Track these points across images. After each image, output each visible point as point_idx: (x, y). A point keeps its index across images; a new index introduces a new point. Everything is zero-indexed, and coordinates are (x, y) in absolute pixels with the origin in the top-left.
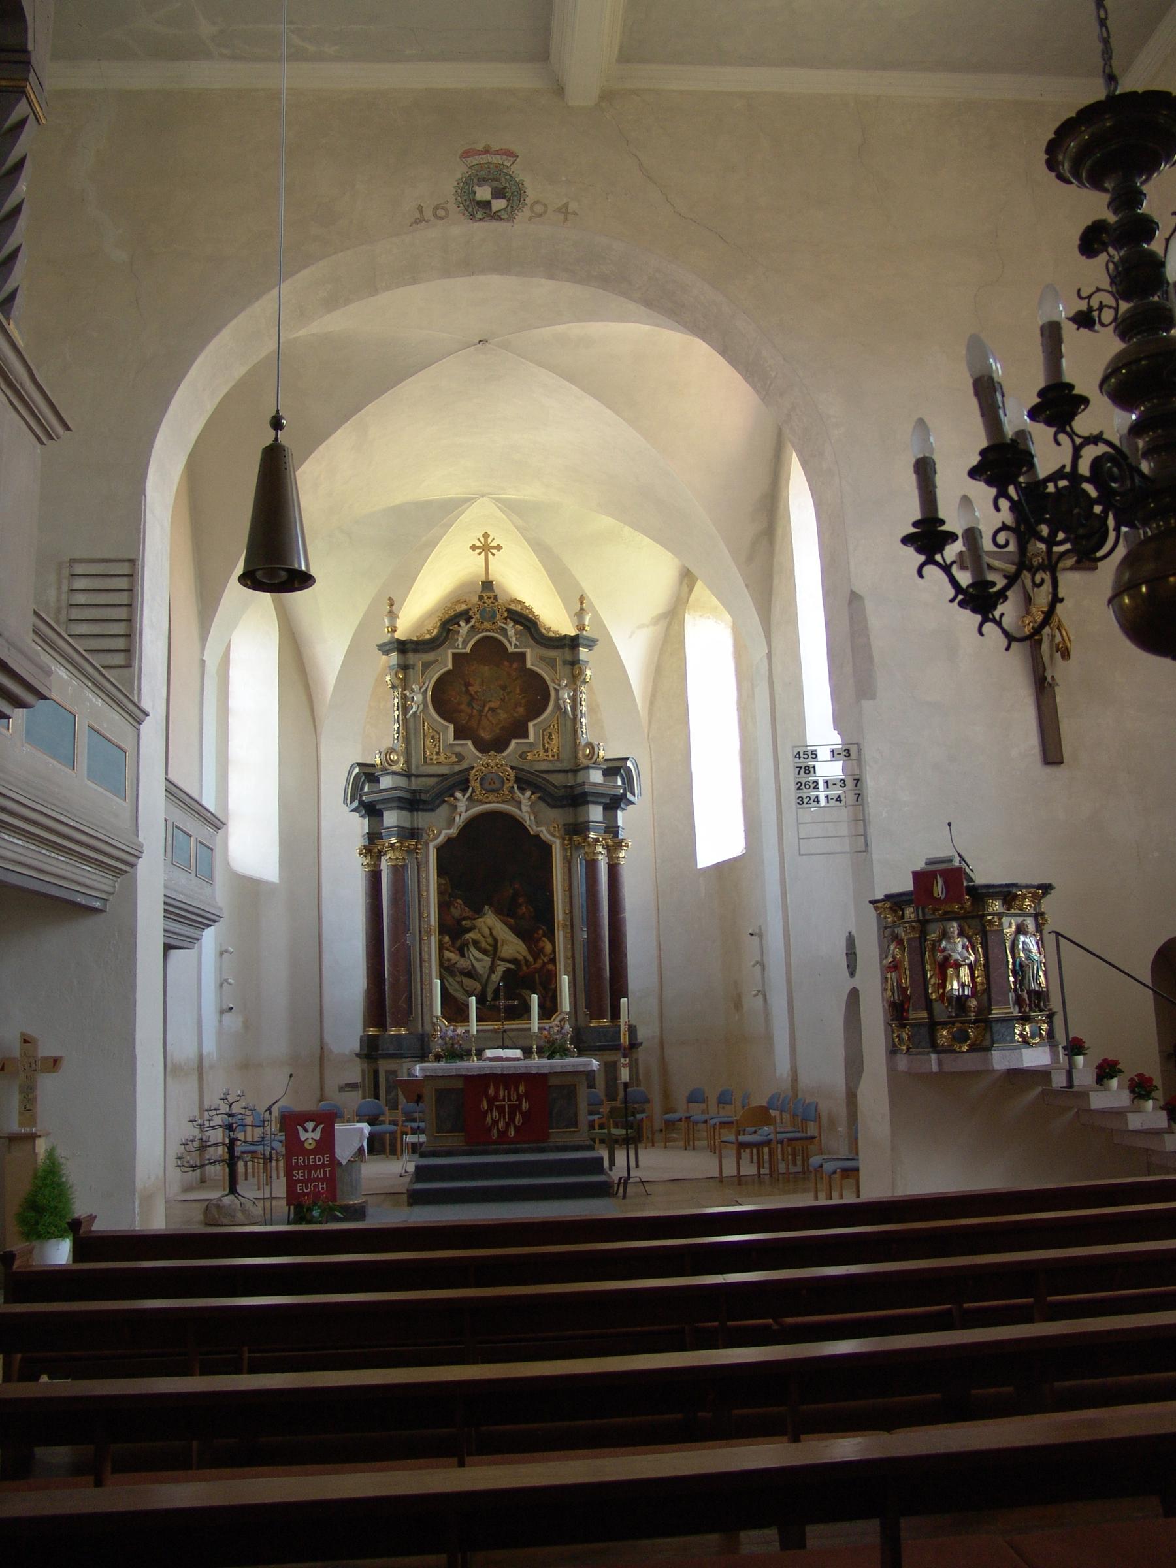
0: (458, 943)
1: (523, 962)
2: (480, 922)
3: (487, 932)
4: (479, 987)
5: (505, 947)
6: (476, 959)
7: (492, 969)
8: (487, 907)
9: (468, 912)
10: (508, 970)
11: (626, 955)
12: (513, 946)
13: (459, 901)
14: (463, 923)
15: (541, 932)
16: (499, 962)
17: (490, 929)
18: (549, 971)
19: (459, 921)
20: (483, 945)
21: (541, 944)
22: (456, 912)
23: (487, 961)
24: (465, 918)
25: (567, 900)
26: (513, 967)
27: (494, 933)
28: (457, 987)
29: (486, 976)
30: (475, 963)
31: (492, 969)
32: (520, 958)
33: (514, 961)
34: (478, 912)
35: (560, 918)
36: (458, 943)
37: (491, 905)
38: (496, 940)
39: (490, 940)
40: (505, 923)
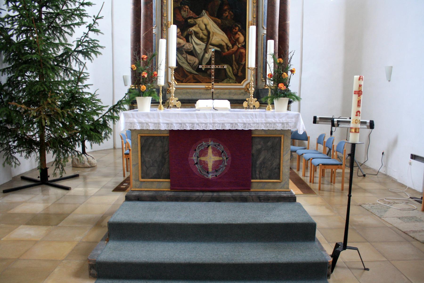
0: (185, 33)
1: (225, 47)
2: (199, 21)
3: (203, 27)
4: (197, 61)
5: (215, 37)
6: (197, 44)
7: (206, 51)
8: (204, 11)
9: (192, 14)
10: (216, 51)
11: (288, 47)
12: (219, 37)
13: (187, 7)
14: (189, 21)
15: (237, 28)
16: (211, 46)
17: (206, 25)
18: (241, 53)
19: (186, 20)
20: (201, 35)
21: (237, 36)
22: (184, 14)
23: (203, 45)
24: (190, 18)
25: (255, 9)
26: (218, 49)
27: (208, 27)
28: (184, 61)
29: (202, 54)
30: (196, 46)
31: (206, 51)
32: (224, 44)
33: (220, 46)
34: (199, 14)
35: (250, 20)
36: (185, 33)
37: (207, 10)
38: (209, 33)
39: (205, 32)
40: (215, 22)
